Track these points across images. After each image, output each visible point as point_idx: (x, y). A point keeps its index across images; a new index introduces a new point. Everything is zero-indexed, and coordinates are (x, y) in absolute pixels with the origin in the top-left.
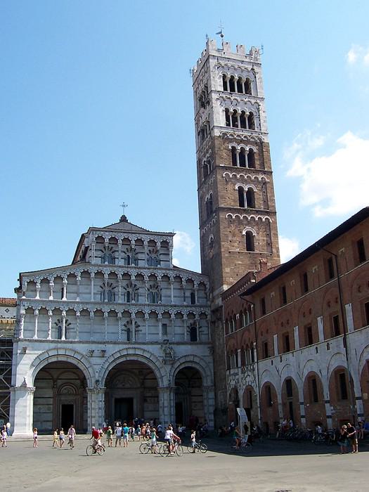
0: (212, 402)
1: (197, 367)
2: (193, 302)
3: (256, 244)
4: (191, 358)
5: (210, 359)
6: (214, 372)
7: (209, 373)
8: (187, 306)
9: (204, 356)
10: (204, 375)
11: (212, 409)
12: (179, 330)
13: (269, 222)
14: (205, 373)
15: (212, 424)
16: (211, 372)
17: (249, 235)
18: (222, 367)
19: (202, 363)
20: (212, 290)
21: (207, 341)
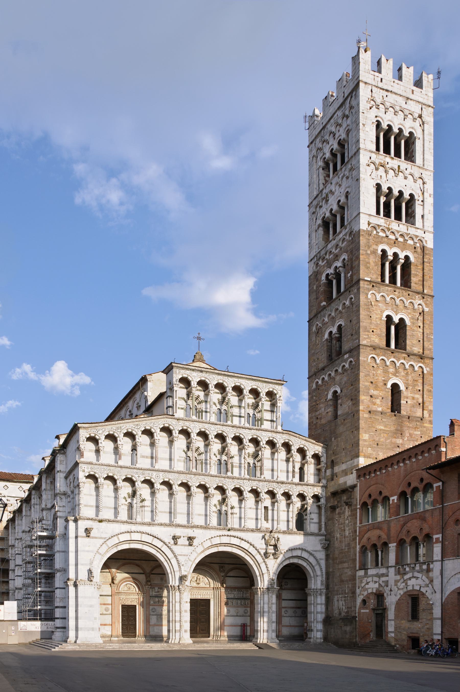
0: (321, 608)
1: (305, 564)
2: (302, 478)
3: (403, 402)
4: (298, 553)
5: (321, 555)
6: (328, 574)
7: (319, 573)
8: (296, 484)
9: (316, 551)
10: (312, 575)
11: (321, 617)
12: (285, 515)
13: (423, 372)
14: (314, 570)
15: (319, 635)
16: (321, 569)
17: (395, 387)
18: (346, 565)
19: (311, 560)
20: (333, 464)
21: (316, 531)
